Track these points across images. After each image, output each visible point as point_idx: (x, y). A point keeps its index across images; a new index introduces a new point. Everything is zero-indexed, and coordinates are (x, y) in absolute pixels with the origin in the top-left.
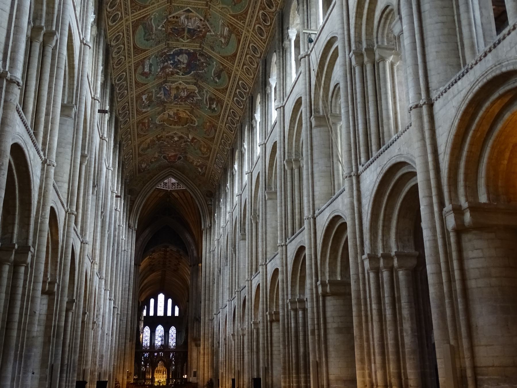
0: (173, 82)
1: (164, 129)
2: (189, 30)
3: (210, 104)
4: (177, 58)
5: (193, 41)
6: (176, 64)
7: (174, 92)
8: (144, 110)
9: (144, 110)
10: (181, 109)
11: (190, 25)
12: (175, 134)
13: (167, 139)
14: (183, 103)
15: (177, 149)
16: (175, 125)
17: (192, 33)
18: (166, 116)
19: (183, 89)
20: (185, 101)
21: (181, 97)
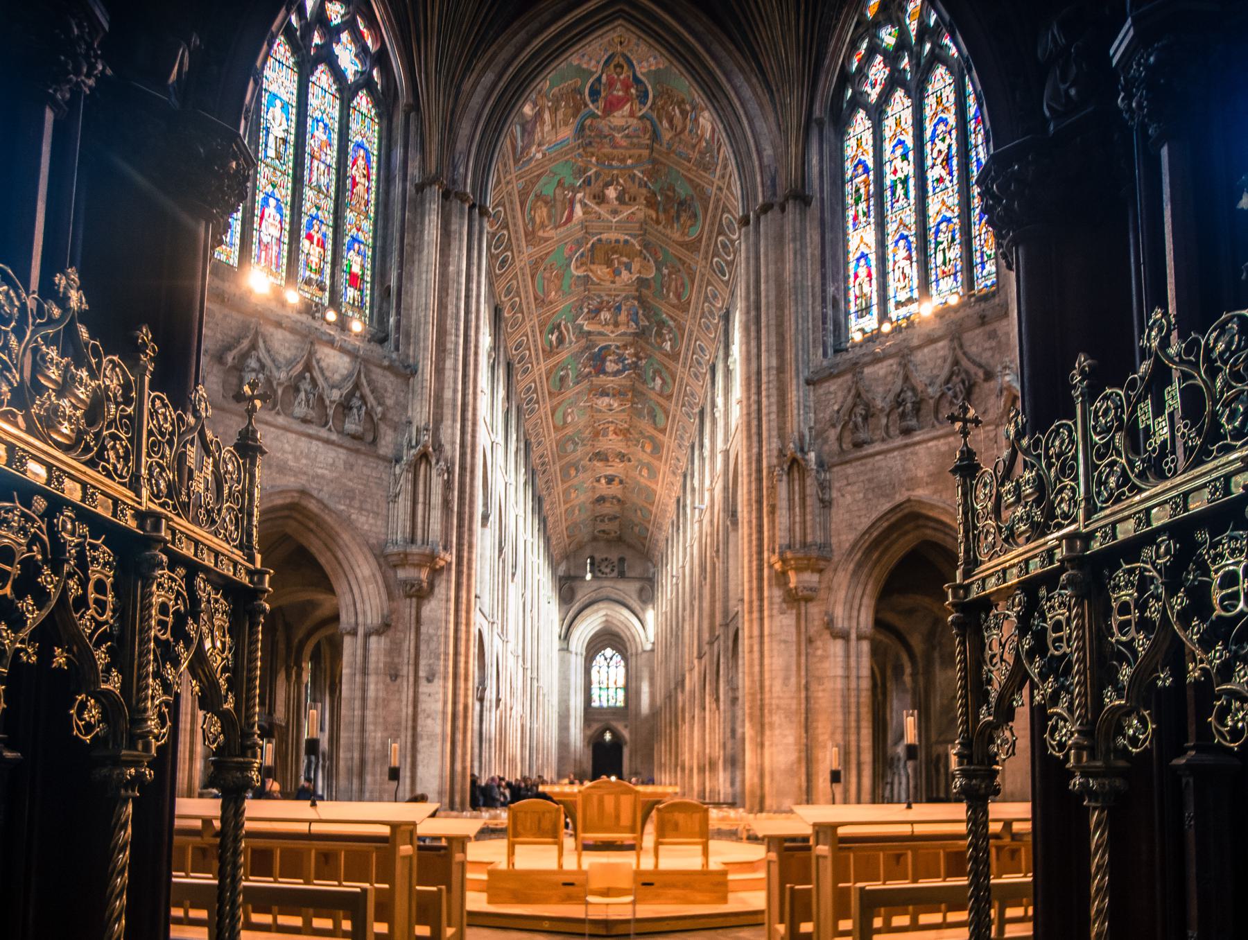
0: (624, 334)
1: (641, 228)
2: (608, 395)
3: (561, 333)
4: (620, 366)
5: (601, 386)
6: (621, 359)
7: (623, 317)
8: (671, 323)
9: (671, 323)
10: (608, 285)
11: (606, 400)
12: (615, 212)
13: (634, 189)
14: (606, 298)
15: (607, 150)
16: (617, 241)
17: (604, 393)
18: (636, 266)
19: (607, 324)
20: (602, 302)
21: (609, 310)
